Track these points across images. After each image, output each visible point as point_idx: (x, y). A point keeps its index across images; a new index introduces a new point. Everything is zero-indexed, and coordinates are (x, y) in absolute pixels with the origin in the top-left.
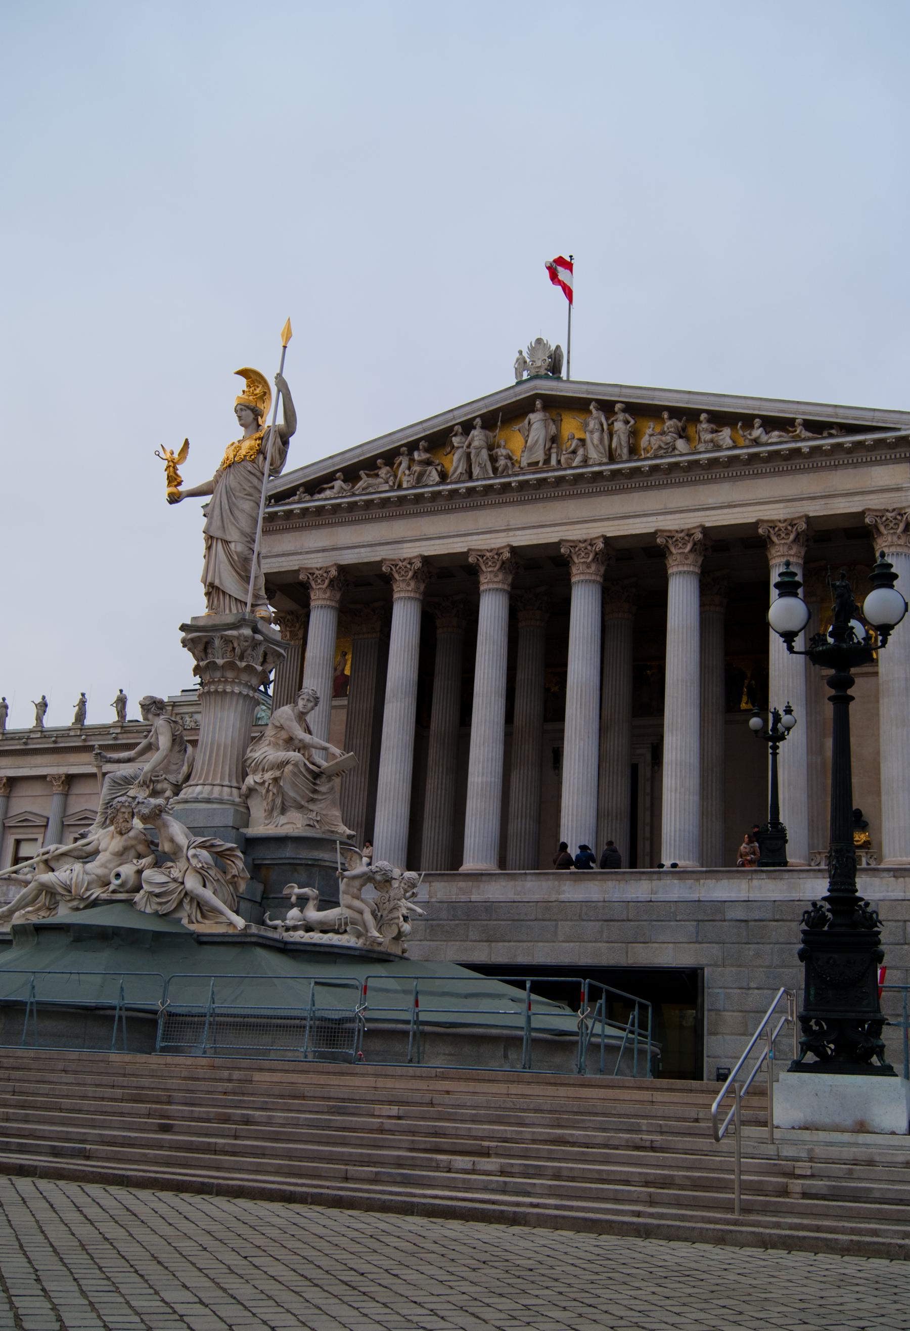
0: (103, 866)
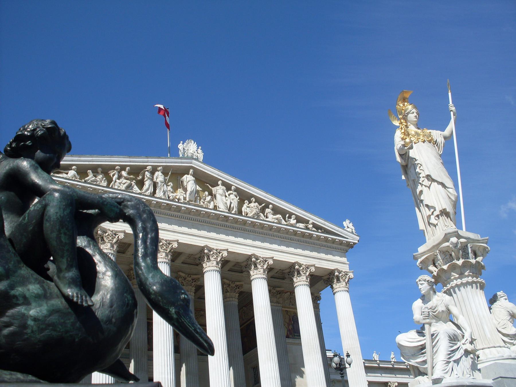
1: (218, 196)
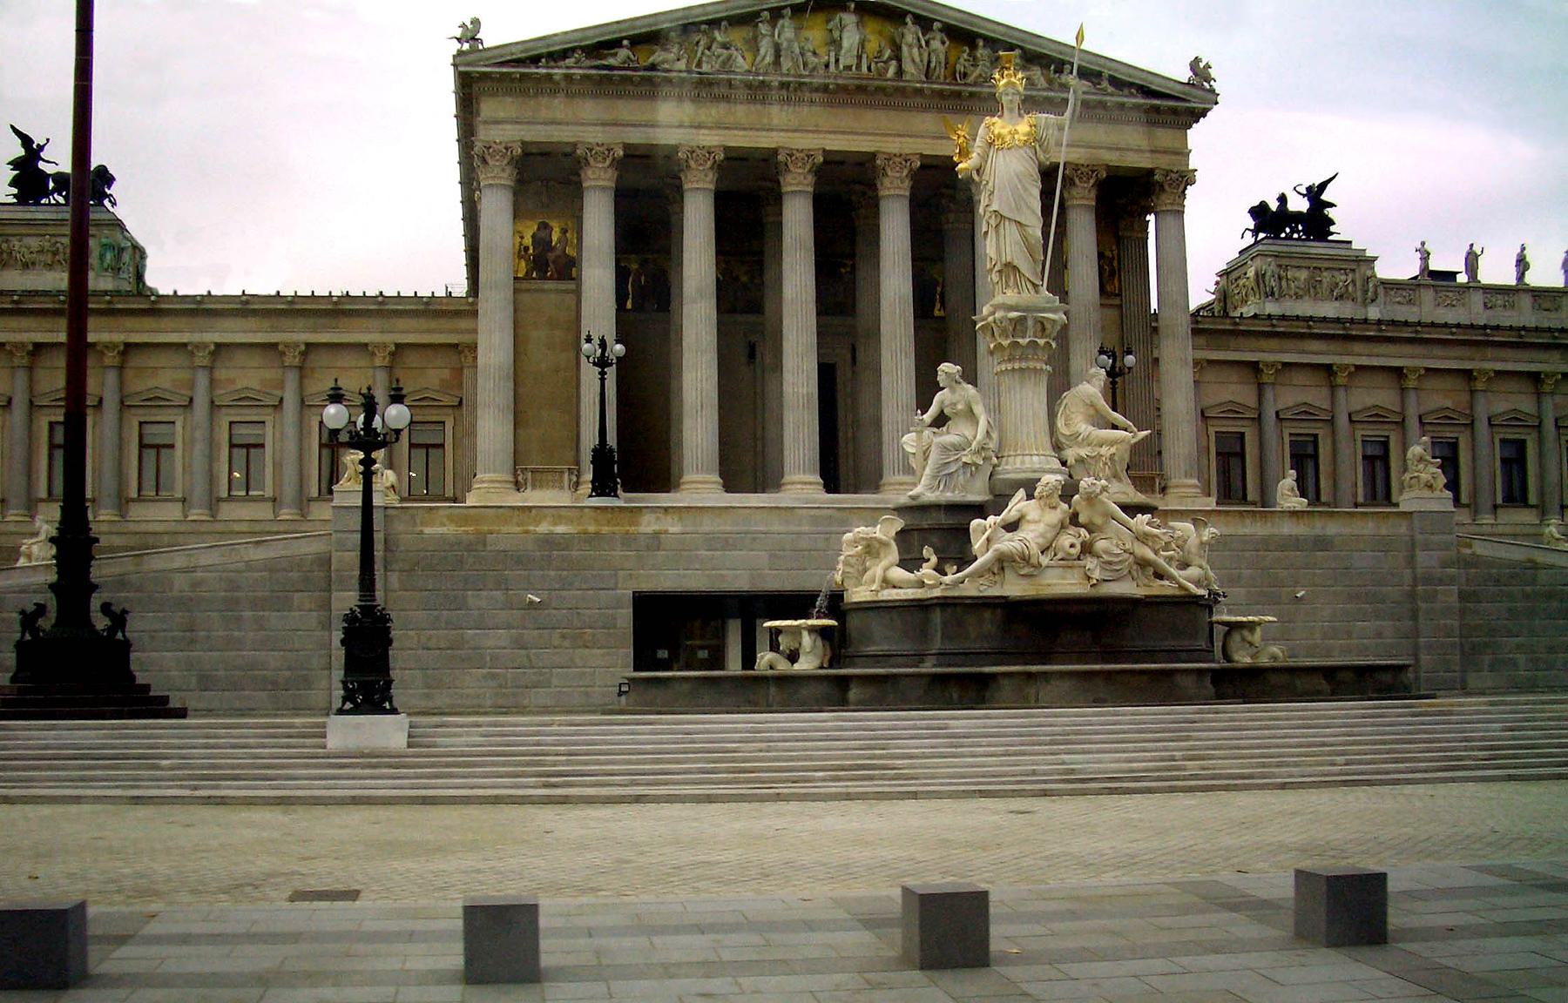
0: (1042, 535)
1: (905, 49)
